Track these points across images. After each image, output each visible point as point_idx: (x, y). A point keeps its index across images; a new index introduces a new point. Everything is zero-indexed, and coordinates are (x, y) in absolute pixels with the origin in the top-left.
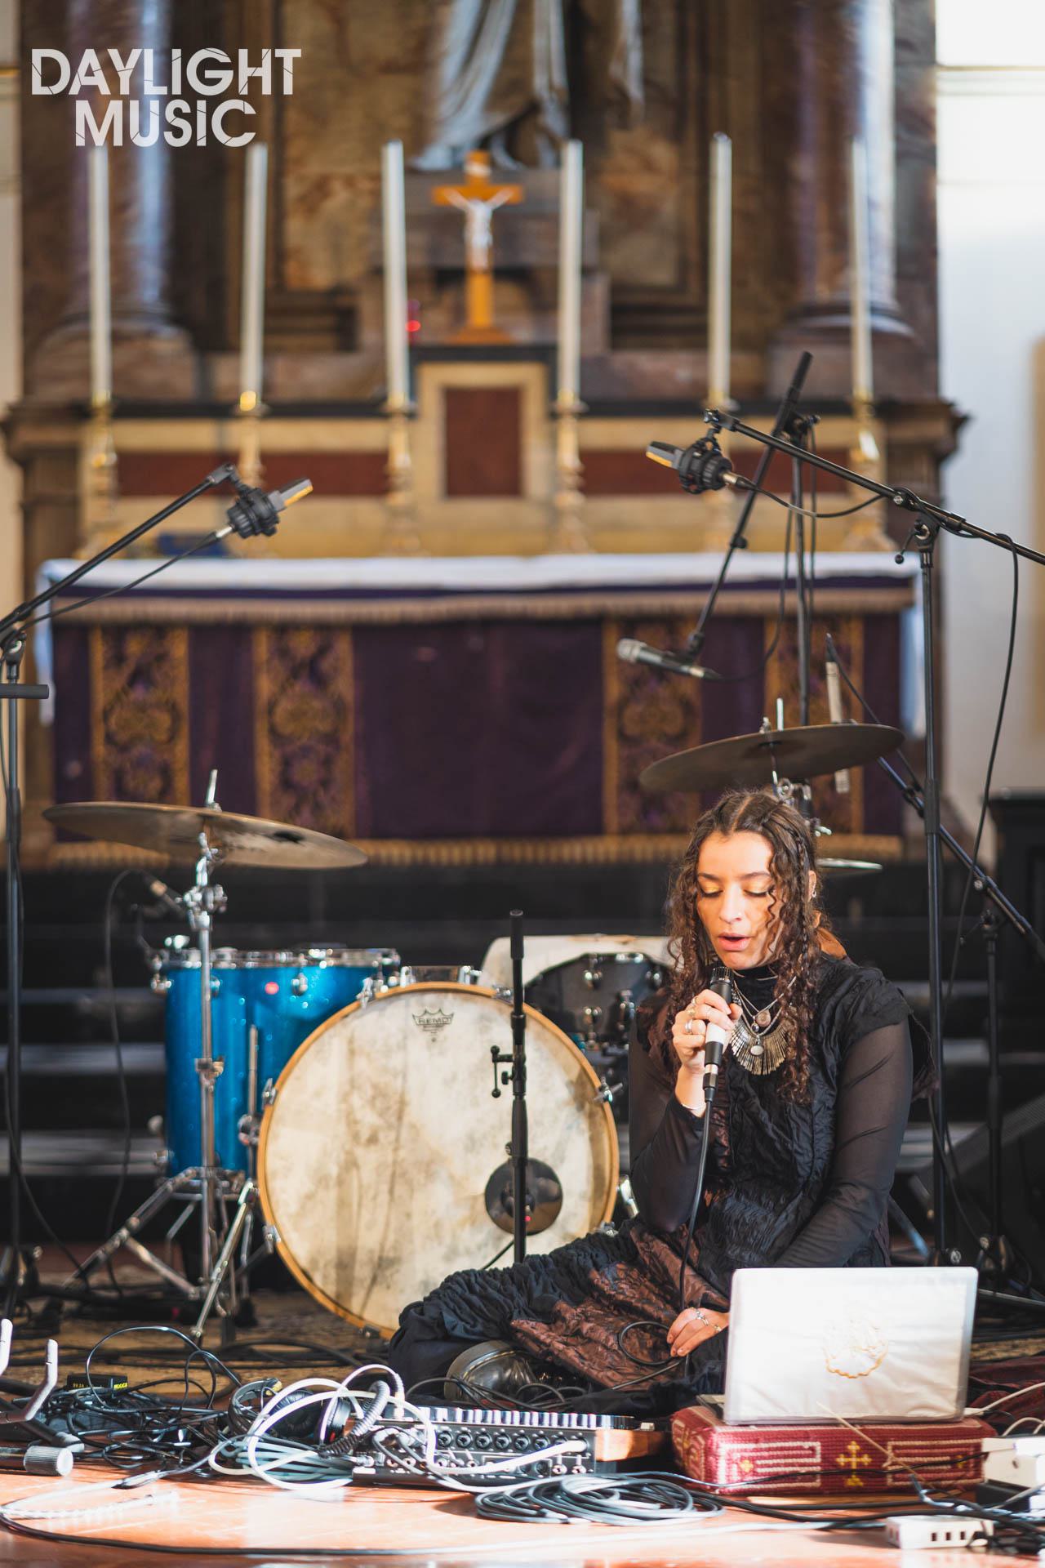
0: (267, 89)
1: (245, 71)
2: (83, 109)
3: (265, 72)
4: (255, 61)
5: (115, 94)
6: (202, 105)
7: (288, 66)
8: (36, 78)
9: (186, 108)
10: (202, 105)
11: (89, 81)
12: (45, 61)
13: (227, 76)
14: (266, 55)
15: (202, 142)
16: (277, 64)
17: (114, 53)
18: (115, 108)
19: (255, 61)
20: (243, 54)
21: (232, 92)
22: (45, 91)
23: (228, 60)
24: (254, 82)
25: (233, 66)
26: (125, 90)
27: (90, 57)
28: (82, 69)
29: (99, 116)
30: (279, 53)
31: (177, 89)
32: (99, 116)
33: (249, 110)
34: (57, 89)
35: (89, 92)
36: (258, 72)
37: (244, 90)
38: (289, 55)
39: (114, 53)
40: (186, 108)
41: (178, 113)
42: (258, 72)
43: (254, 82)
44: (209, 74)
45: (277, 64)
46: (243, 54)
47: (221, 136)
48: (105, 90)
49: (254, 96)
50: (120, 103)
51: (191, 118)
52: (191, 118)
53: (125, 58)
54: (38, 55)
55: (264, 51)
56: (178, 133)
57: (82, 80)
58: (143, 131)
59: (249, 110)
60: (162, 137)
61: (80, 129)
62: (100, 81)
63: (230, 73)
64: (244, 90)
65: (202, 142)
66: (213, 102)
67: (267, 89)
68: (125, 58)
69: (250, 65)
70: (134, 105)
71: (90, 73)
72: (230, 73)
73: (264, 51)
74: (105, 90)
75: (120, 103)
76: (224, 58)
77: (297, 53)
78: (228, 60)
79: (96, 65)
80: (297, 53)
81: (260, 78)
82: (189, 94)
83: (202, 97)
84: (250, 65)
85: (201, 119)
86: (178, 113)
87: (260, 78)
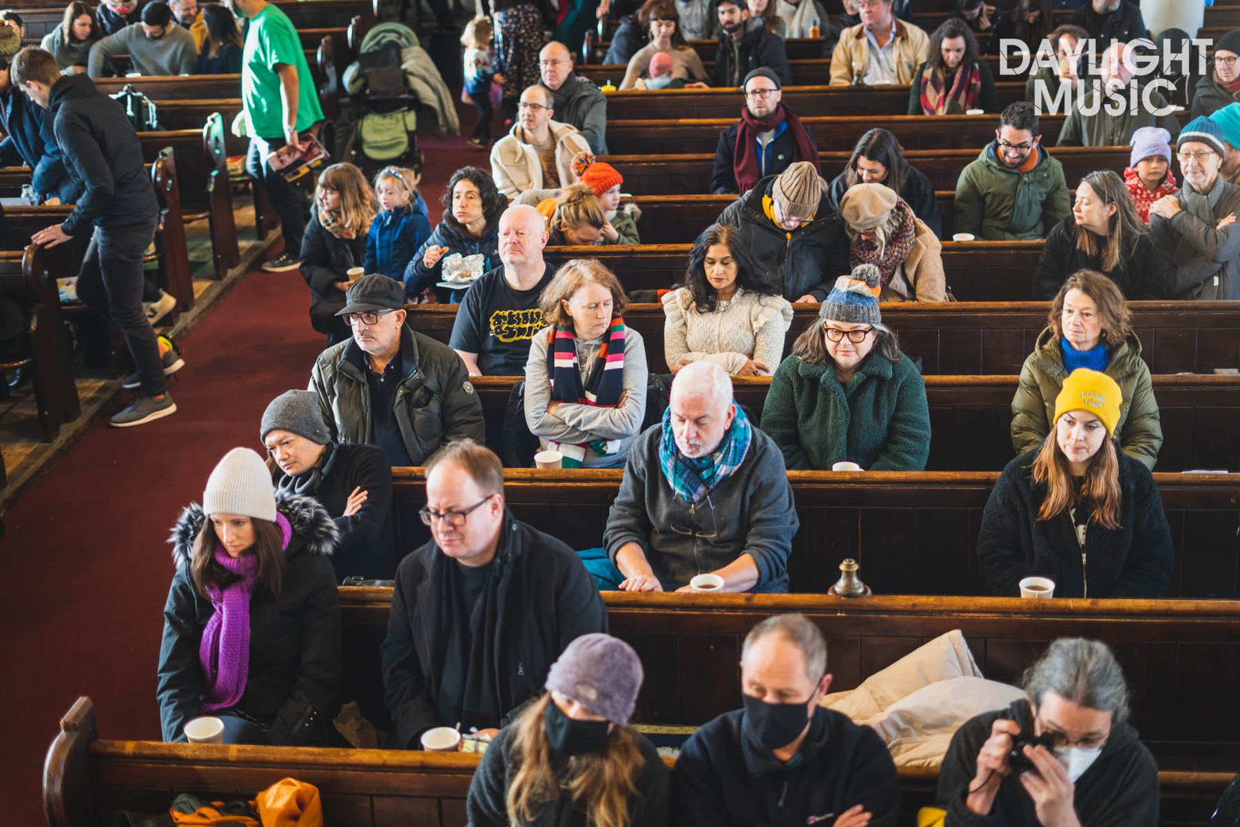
0: (1186, 71)
1: (1169, 57)
2: (1041, 87)
3: (1184, 57)
7: (1203, 52)
11: (1046, 64)
12: (1012, 49)
13: (1154, 61)
15: (1134, 113)
21: (1159, 71)
22: (1011, 72)
23: (1155, 47)
24: (1176, 65)
25: (1160, 52)
28: (1040, 54)
33: (1172, 87)
34: (1020, 70)
36: (1179, 57)
37: (1167, 71)
42: (1179, 57)
43: (1176, 65)
49: (1176, 76)
52: (1125, 93)
54: (1004, 43)
56: (1114, 104)
58: (1089, 103)
59: (1172, 87)
61: (1038, 102)
63: (1157, 58)
64: (1167, 71)
65: (1134, 113)
66: (1143, 81)
67: (1186, 71)
72: (1157, 58)
78: (1155, 47)
81: (1179, 63)
87: (1179, 63)
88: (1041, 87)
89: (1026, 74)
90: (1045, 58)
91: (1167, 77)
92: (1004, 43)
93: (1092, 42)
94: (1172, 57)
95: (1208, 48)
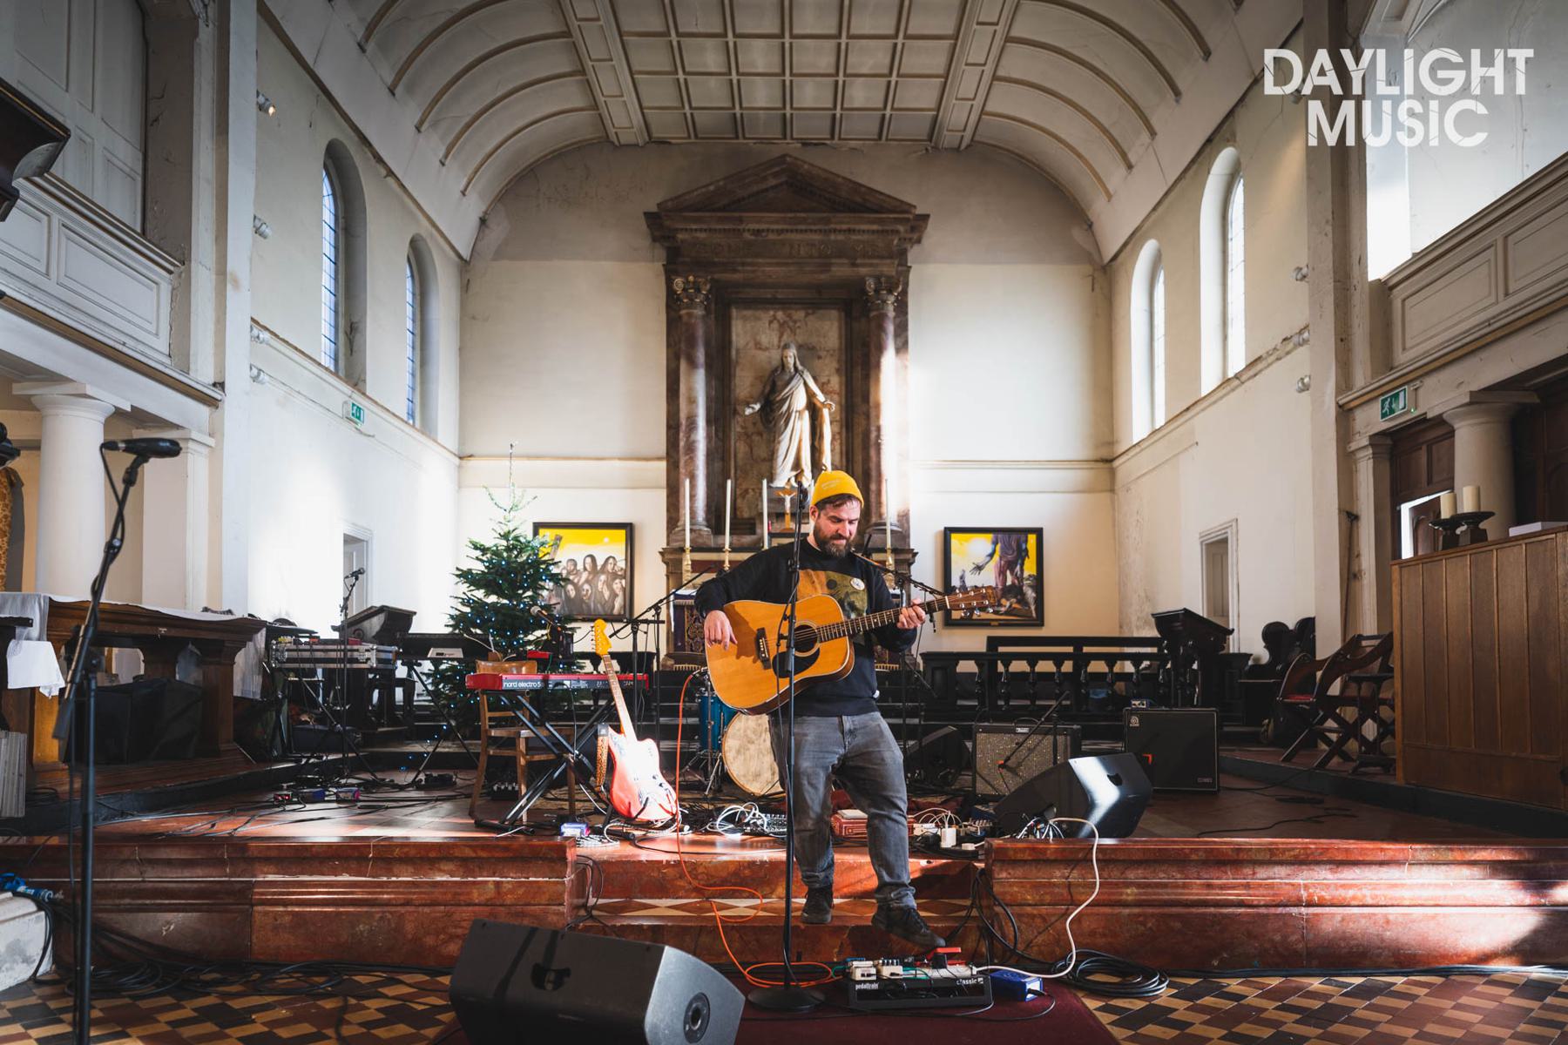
0: (1499, 89)
1: (1478, 71)
3: (1497, 71)
4: (1487, 61)
5: (1347, 94)
6: (1434, 105)
8: (1269, 78)
9: (1418, 108)
10: (1434, 105)
13: (1459, 76)
14: (1499, 54)
15: (1434, 142)
16: (1510, 64)
17: (1347, 54)
18: (1348, 107)
19: (1487, 61)
20: (1476, 54)
21: (1465, 91)
22: (1278, 91)
23: (1460, 60)
24: (1487, 82)
25: (1466, 66)
26: (1357, 89)
27: (1322, 57)
28: (1315, 69)
29: (1332, 114)
30: (1512, 53)
31: (1409, 89)
32: (1332, 114)
34: (1289, 89)
35: (1321, 92)
37: (1476, 89)
38: (1521, 55)
39: (1347, 54)
40: (1418, 108)
41: (1411, 113)
42: (1491, 72)
44: (1442, 74)
45: (1510, 64)
46: (1476, 54)
47: (1453, 135)
48: (1337, 90)
49: (1487, 95)
50: (1352, 103)
51: (1424, 118)
52: (1424, 118)
53: (1357, 60)
54: (1269, 55)
55: (1497, 51)
57: (1315, 79)
59: (1482, 110)
60: (1394, 136)
61: (1313, 129)
62: (1331, 80)
65: (1434, 142)
66: (1445, 102)
67: (1499, 89)
68: (1357, 60)
69: (1482, 65)
70: (1367, 105)
71: (1322, 72)
73: (1497, 51)
74: (1337, 90)
75: (1352, 103)
76: (1455, 58)
77: (1530, 53)
78: (1460, 60)
79: (1328, 65)
80: (1530, 53)
82: (1422, 95)
83: (1434, 97)
84: (1482, 65)
85: (1434, 118)
86: (1411, 113)
88: (1316, 109)
89: (1297, 95)
90: (1322, 72)
91: (1476, 98)
92: (1269, 55)
93: (1381, 53)
94: (1483, 71)
95: (1527, 60)
